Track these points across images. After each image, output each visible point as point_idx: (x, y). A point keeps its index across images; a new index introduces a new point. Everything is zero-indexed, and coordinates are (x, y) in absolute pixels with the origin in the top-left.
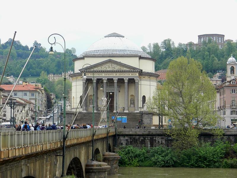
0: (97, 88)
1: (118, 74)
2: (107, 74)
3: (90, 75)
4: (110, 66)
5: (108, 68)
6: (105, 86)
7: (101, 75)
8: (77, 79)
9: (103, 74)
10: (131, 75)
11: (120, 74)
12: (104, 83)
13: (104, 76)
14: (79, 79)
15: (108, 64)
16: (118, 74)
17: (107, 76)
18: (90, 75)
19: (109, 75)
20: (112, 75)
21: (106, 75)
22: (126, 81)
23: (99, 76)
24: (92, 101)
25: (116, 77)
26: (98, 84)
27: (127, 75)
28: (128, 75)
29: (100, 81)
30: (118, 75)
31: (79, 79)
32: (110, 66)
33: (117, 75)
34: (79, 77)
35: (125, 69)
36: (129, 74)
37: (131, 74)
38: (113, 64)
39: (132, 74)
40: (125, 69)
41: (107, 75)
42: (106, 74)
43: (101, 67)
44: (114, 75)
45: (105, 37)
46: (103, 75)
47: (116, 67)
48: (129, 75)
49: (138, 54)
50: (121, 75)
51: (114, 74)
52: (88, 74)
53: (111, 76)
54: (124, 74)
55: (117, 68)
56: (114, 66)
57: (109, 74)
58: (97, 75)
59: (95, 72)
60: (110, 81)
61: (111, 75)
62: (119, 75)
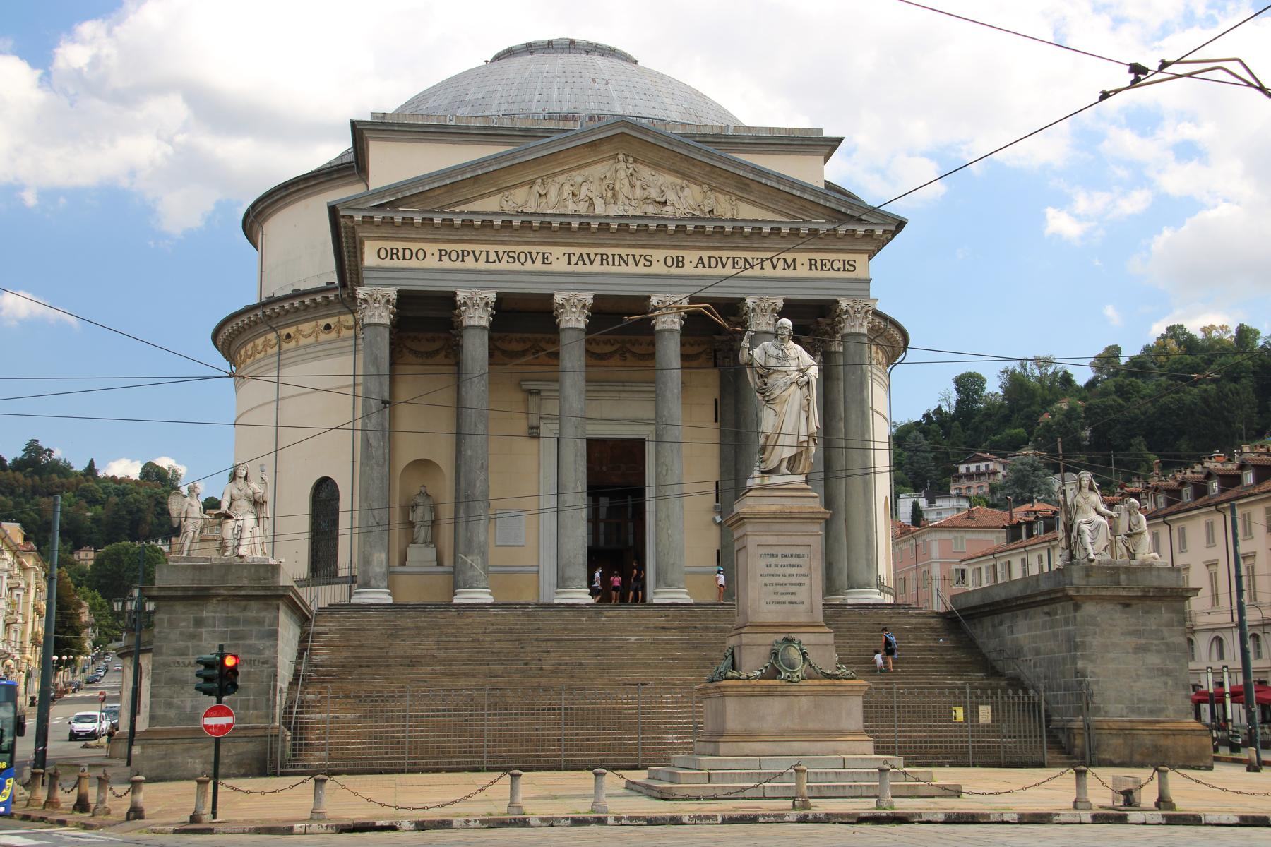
2: (592, 251)
3: (430, 262)
5: (599, 203)
6: (573, 356)
7: (538, 266)
8: (293, 344)
9: (558, 252)
10: (803, 271)
11: (705, 254)
12: (566, 338)
13: (573, 278)
14: (303, 341)
16: (691, 256)
17: (588, 268)
18: (432, 262)
19: (605, 269)
20: (640, 269)
21: (581, 268)
24: (428, 517)
25: (669, 280)
27: (768, 271)
28: (780, 272)
30: (689, 269)
31: (303, 341)
32: (623, 187)
33: (679, 262)
34: (307, 327)
35: (747, 212)
36: (789, 257)
37: (803, 258)
38: (645, 172)
39: (812, 264)
40: (747, 212)
41: (596, 267)
42: (584, 251)
43: (537, 188)
44: (659, 260)
45: (497, 58)
46: (559, 259)
47: (671, 196)
48: (790, 273)
49: (820, 131)
50: (719, 271)
51: (659, 255)
52: (415, 246)
55: (686, 199)
56: (659, 182)
57: (610, 251)
58: (504, 266)
59: (486, 228)
60: (621, 327)
61: (632, 269)
62: (701, 271)
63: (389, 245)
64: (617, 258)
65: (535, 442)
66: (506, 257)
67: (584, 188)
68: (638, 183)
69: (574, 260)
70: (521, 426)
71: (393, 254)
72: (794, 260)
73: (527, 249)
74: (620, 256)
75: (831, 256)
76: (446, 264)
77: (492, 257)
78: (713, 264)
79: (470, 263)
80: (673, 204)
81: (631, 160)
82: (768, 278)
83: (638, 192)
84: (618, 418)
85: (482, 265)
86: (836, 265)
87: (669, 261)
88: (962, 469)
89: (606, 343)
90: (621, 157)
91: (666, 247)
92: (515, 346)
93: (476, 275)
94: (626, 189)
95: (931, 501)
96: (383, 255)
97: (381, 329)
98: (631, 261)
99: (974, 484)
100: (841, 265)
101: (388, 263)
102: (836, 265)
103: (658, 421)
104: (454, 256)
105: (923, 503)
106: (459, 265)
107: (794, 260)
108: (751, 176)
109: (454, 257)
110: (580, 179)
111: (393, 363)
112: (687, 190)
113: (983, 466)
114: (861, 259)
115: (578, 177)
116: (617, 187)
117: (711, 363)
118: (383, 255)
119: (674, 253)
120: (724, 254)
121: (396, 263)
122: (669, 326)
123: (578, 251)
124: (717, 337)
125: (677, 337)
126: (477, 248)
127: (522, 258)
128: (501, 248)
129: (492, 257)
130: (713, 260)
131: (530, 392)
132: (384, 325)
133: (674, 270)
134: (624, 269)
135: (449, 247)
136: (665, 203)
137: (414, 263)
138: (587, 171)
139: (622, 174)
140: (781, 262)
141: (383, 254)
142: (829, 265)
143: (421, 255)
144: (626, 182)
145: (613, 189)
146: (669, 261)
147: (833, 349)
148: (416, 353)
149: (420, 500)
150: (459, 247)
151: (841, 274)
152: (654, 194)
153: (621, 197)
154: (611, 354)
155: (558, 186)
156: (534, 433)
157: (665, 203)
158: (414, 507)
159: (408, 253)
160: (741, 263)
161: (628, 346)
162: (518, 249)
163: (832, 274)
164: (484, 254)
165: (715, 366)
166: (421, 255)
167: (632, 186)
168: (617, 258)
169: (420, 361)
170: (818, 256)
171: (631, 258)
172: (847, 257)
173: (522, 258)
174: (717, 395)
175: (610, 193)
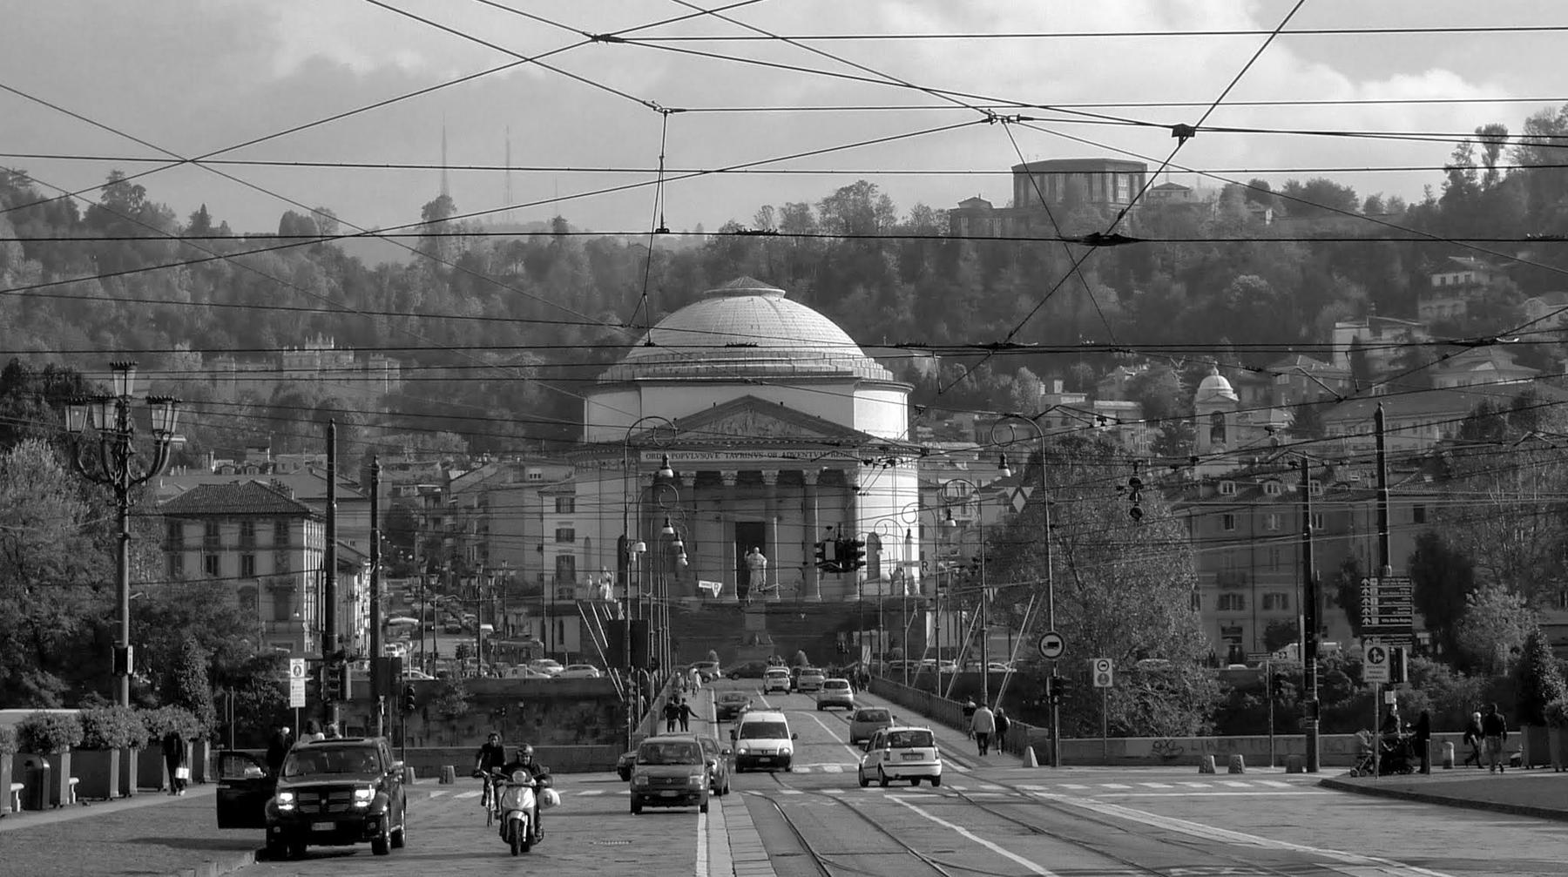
4: (750, 422)
13: (726, 462)
15: (740, 416)
22: (812, 481)
25: (769, 462)
29: (708, 479)
32: (750, 422)
34: (613, 461)
35: (806, 433)
40: (806, 433)
41: (739, 458)
44: (765, 455)
51: (765, 452)
53: (751, 459)
55: (776, 429)
56: (765, 420)
60: (750, 479)
82: (812, 462)
88: (1436, 280)
95: (1376, 331)
99: (1449, 303)
105: (1365, 335)
113: (1462, 277)
115: (730, 419)
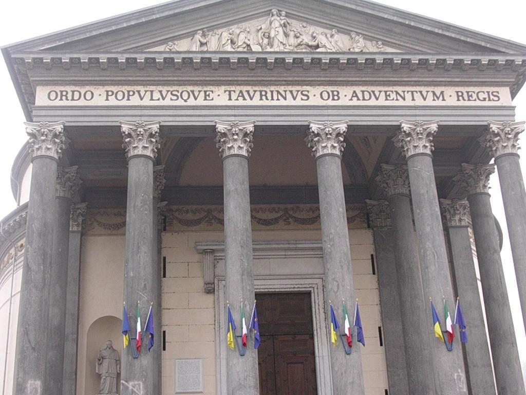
0: (161, 268)
1: (346, 96)
3: (99, 102)
7: (201, 101)
10: (451, 101)
11: (358, 90)
13: (232, 110)
17: (249, 102)
20: (299, 102)
21: (241, 102)
23: (180, 102)
25: (328, 110)
26: (163, 234)
27: (419, 102)
28: (430, 102)
30: (344, 101)
33: (335, 96)
36: (438, 90)
37: (450, 91)
38: (296, 25)
39: (459, 96)
41: (256, 101)
42: (244, 88)
43: (198, 37)
44: (315, 96)
47: (322, 39)
48: (439, 103)
50: (373, 102)
54: (400, 89)
58: (167, 102)
62: (355, 102)
63: (58, 89)
64: (275, 94)
65: (210, 298)
66: (169, 95)
67: (242, 36)
68: (292, 34)
69: (234, 96)
70: (200, 284)
71: (64, 95)
72: (442, 93)
73: (190, 88)
74: (278, 92)
75: (477, 89)
76: (112, 102)
77: (156, 95)
78: (367, 97)
79: (135, 101)
80: (325, 46)
81: (283, 13)
82: (419, 109)
83: (292, 41)
84: (285, 274)
85: (147, 102)
86: (481, 96)
87: (325, 95)
89: (273, 210)
90: (274, 11)
91: (321, 83)
92: (190, 216)
93: (142, 110)
94: (281, 37)
96: (53, 97)
97: (48, 160)
98: (289, 96)
100: (486, 96)
101: (58, 103)
102: (481, 96)
103: (323, 277)
104: (120, 96)
106: (124, 103)
107: (442, 93)
108: (395, 19)
109: (120, 96)
110: (238, 31)
111: (83, 234)
112: (336, 37)
114: (504, 93)
115: (235, 29)
116: (272, 35)
117: (366, 225)
118: (53, 97)
119: (329, 89)
120: (376, 89)
121: (65, 103)
122: (329, 151)
123: (238, 88)
124: (368, 201)
125: (338, 161)
126: (142, 89)
127: (185, 96)
128: (164, 89)
129: (156, 95)
130: (367, 96)
131: (205, 252)
132: (51, 158)
133: (330, 102)
134: (282, 102)
135: (115, 89)
136: (317, 47)
137: (82, 102)
138: (244, 25)
139: (277, 24)
140: (430, 94)
141: (53, 96)
142: (475, 96)
143: (89, 96)
144: (280, 30)
145: (269, 37)
146: (325, 95)
147: (478, 191)
148: (105, 226)
149: (105, 353)
150: (125, 88)
151: (487, 103)
152: (306, 39)
153: (276, 43)
154: (276, 221)
155: (217, 37)
156: (210, 290)
157: (317, 47)
158: (101, 359)
159: (76, 95)
160: (393, 96)
161: (291, 213)
162: (180, 89)
163: (478, 103)
164: (149, 94)
165: (369, 227)
166: (89, 96)
167: (286, 35)
168: (275, 94)
169: (109, 232)
170: (464, 89)
171: (288, 93)
172: (491, 89)
173: (185, 96)
174: (371, 250)
175: (266, 41)
